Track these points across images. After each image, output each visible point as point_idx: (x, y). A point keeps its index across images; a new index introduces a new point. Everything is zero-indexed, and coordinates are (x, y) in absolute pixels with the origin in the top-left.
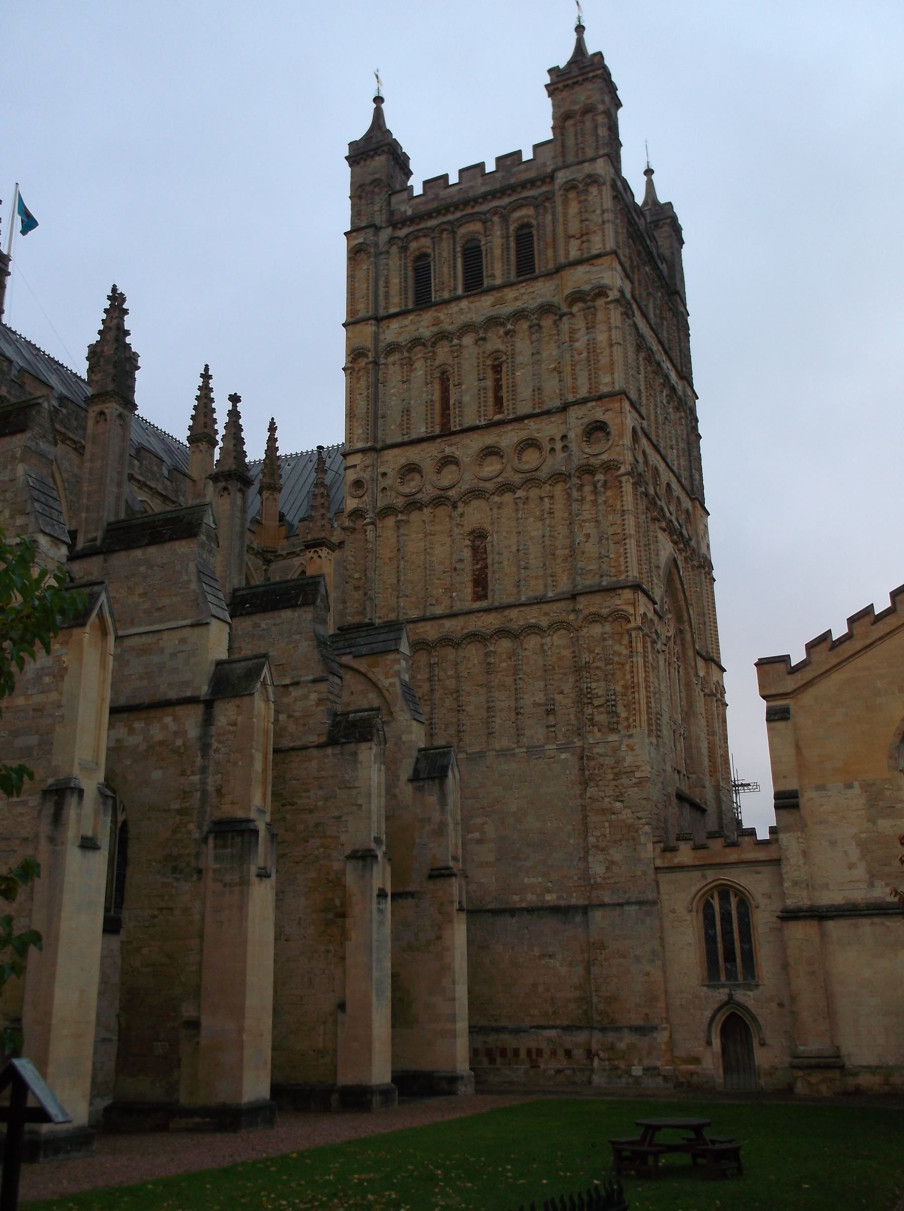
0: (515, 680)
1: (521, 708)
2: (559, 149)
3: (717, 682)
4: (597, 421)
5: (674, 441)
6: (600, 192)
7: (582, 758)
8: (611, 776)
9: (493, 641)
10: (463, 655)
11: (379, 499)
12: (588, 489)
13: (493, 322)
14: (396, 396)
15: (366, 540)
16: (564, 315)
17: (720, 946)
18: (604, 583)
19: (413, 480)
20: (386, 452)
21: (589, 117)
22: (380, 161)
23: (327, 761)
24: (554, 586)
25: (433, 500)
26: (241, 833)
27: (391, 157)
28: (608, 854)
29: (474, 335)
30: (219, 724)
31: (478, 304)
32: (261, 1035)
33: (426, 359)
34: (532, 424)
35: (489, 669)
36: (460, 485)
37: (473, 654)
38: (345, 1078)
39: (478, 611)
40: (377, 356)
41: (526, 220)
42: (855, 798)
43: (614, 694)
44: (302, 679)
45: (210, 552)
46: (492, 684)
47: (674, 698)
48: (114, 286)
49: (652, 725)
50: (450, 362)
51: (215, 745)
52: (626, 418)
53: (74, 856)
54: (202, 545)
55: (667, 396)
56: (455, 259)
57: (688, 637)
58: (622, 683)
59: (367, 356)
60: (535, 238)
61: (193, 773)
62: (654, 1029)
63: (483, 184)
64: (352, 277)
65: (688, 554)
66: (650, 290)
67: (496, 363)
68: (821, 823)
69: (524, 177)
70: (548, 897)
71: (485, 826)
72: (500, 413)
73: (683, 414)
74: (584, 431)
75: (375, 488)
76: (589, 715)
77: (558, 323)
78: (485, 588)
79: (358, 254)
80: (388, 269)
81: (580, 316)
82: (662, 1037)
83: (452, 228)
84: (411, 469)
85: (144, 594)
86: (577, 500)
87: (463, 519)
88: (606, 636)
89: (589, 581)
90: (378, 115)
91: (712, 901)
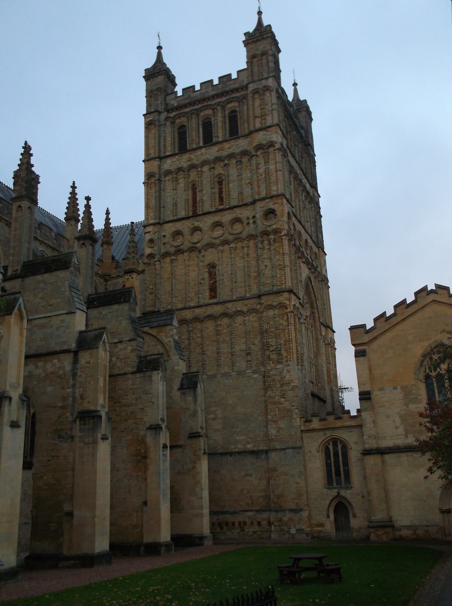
0: (231, 338)
1: (234, 352)
2: (250, 73)
3: (331, 337)
4: (270, 209)
5: (308, 219)
6: (271, 95)
7: (264, 377)
8: (279, 386)
9: (220, 319)
10: (205, 326)
11: (162, 248)
12: (266, 243)
13: (218, 159)
14: (170, 197)
15: (156, 269)
16: (253, 156)
17: (333, 468)
18: (274, 290)
19: (179, 239)
20: (165, 225)
21: (264, 57)
22: (160, 79)
23: (136, 380)
24: (249, 291)
25: (190, 248)
26: (93, 417)
27: (166, 77)
28: (278, 424)
29: (208, 166)
30: (81, 363)
31: (210, 150)
32: (104, 519)
33: (185, 178)
34: (238, 210)
35: (218, 333)
36: (202, 241)
37: (210, 326)
38: (147, 539)
39: (212, 304)
40: (160, 176)
41: (234, 109)
42: (398, 394)
43: (280, 345)
44: (124, 339)
45: (75, 276)
46: (220, 341)
47: (310, 346)
48: (26, 142)
49: (299, 359)
50: (197, 180)
51: (79, 373)
52: (284, 207)
53: (7, 430)
54: (72, 273)
55: (305, 196)
56: (199, 128)
57: (317, 316)
58: (284, 339)
59: (155, 177)
60: (239, 118)
61: (68, 388)
62: (301, 510)
63: (212, 90)
64: (147, 137)
65: (316, 274)
66: (296, 143)
67: (220, 180)
68: (382, 407)
69: (233, 87)
70: (248, 446)
71: (217, 411)
72: (222, 205)
73: (313, 205)
74: (264, 214)
75: (160, 243)
76: (268, 355)
77: (250, 160)
78: (215, 292)
79: (150, 126)
80: (165, 133)
81: (261, 156)
82: (305, 514)
83: (197, 113)
84: (178, 233)
85: (42, 298)
86: (261, 248)
87: (204, 258)
88: (276, 316)
89: (267, 289)
90: (159, 55)
91: (329, 446)
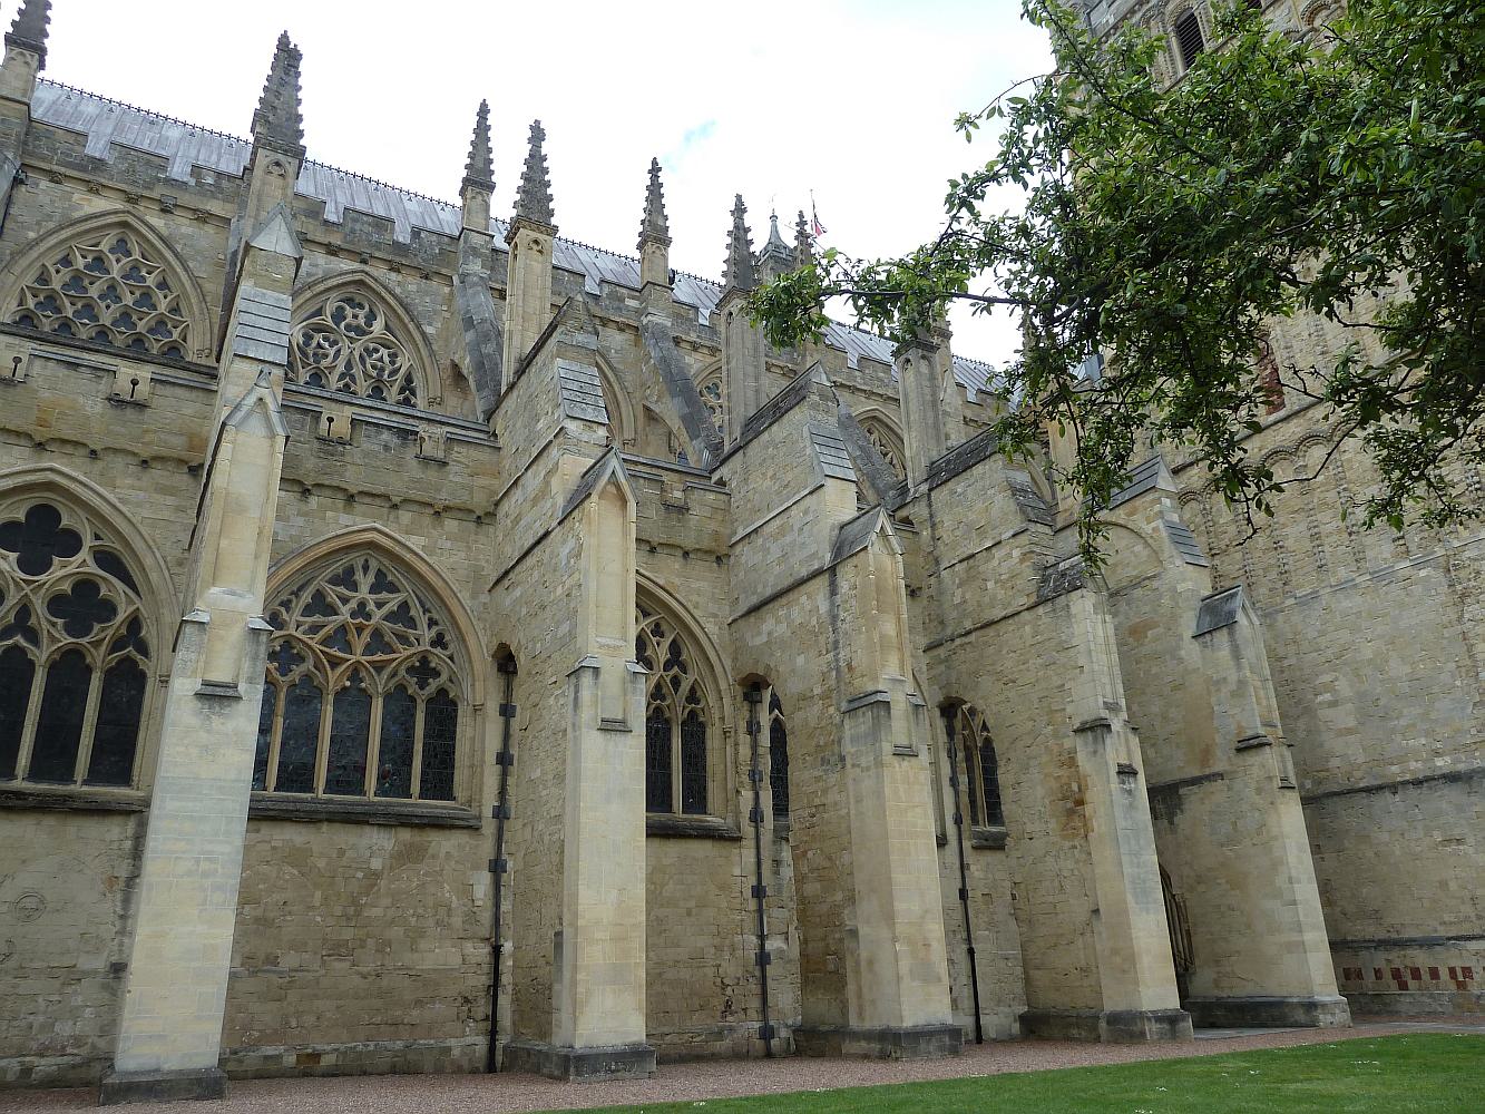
1: (1353, 525)
9: (1301, 454)
38: (1113, 1002)
39: (1276, 423)
44: (1003, 537)
51: (842, 615)
53: (593, 743)
54: (814, 407)
70: (1439, 762)
71: (1336, 683)
